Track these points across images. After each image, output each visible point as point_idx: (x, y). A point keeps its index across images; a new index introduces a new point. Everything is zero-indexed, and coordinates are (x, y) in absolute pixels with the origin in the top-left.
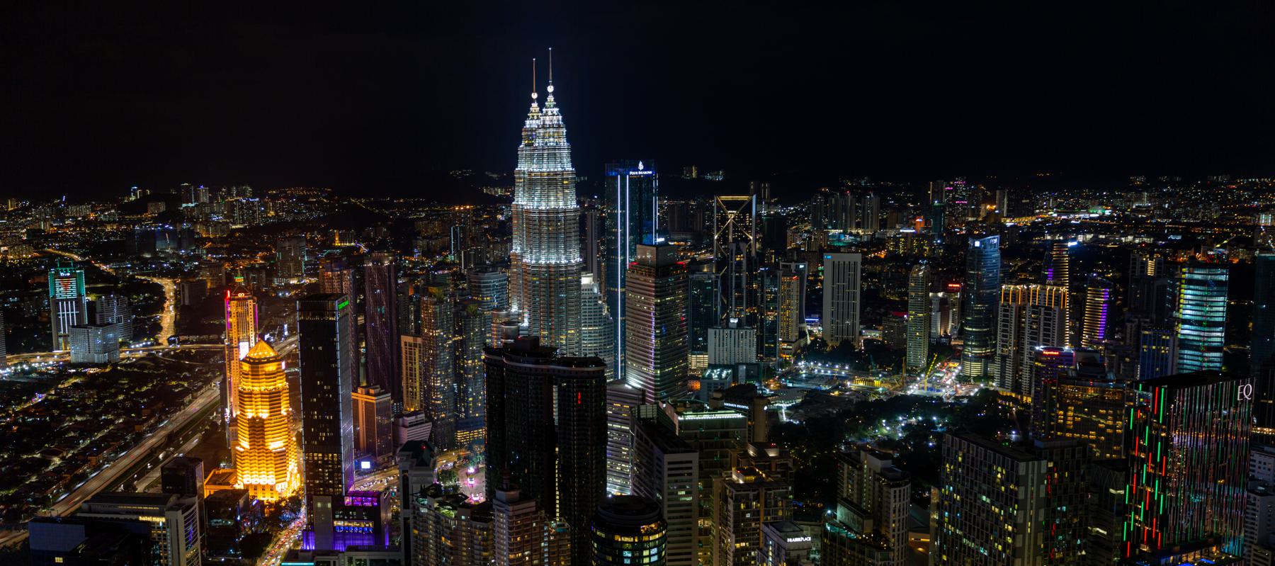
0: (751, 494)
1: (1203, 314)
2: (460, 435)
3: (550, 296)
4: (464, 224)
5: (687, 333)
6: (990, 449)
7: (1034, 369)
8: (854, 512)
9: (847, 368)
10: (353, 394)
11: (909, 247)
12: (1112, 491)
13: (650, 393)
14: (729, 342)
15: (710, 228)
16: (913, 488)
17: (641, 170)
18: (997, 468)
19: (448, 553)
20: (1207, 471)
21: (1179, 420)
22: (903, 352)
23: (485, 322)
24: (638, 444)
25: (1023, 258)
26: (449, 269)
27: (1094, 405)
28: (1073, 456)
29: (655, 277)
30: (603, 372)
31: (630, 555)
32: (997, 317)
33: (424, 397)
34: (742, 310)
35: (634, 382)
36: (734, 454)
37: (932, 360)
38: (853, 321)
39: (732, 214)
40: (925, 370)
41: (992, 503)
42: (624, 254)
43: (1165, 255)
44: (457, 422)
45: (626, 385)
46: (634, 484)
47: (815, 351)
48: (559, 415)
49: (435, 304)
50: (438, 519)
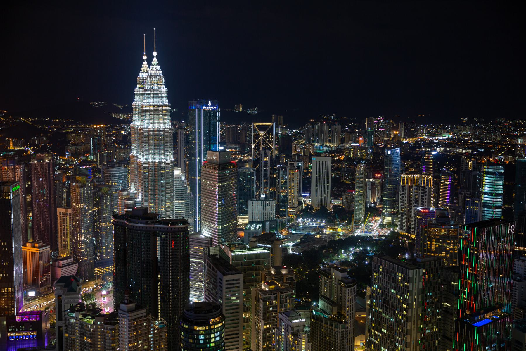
0: (273, 296)
1: (493, 189)
2: (97, 271)
3: (155, 182)
4: (100, 136)
5: (237, 203)
6: (396, 264)
7: (417, 220)
8: (328, 303)
9: (324, 221)
10: (23, 247)
11: (356, 154)
12: (453, 283)
13: (215, 239)
14: (260, 208)
15: (250, 141)
16: (357, 287)
17: (210, 106)
18: (399, 274)
19: (88, 347)
20: (495, 270)
21: (483, 244)
22: (352, 212)
23: (114, 198)
24: (209, 270)
25: (411, 160)
26: (90, 165)
27: (444, 238)
28: (435, 266)
29: (218, 170)
30: (187, 228)
31: (203, 338)
32: (399, 192)
33: (73, 247)
34: (267, 190)
35: (206, 233)
36: (263, 274)
37: (367, 216)
38: (327, 195)
39: (262, 134)
40: (364, 222)
41: (397, 293)
42: (200, 156)
43: (477, 159)
44: (95, 262)
45: (201, 236)
46: (206, 295)
47: (307, 212)
48: (161, 255)
49: (81, 187)
50: (82, 326)
